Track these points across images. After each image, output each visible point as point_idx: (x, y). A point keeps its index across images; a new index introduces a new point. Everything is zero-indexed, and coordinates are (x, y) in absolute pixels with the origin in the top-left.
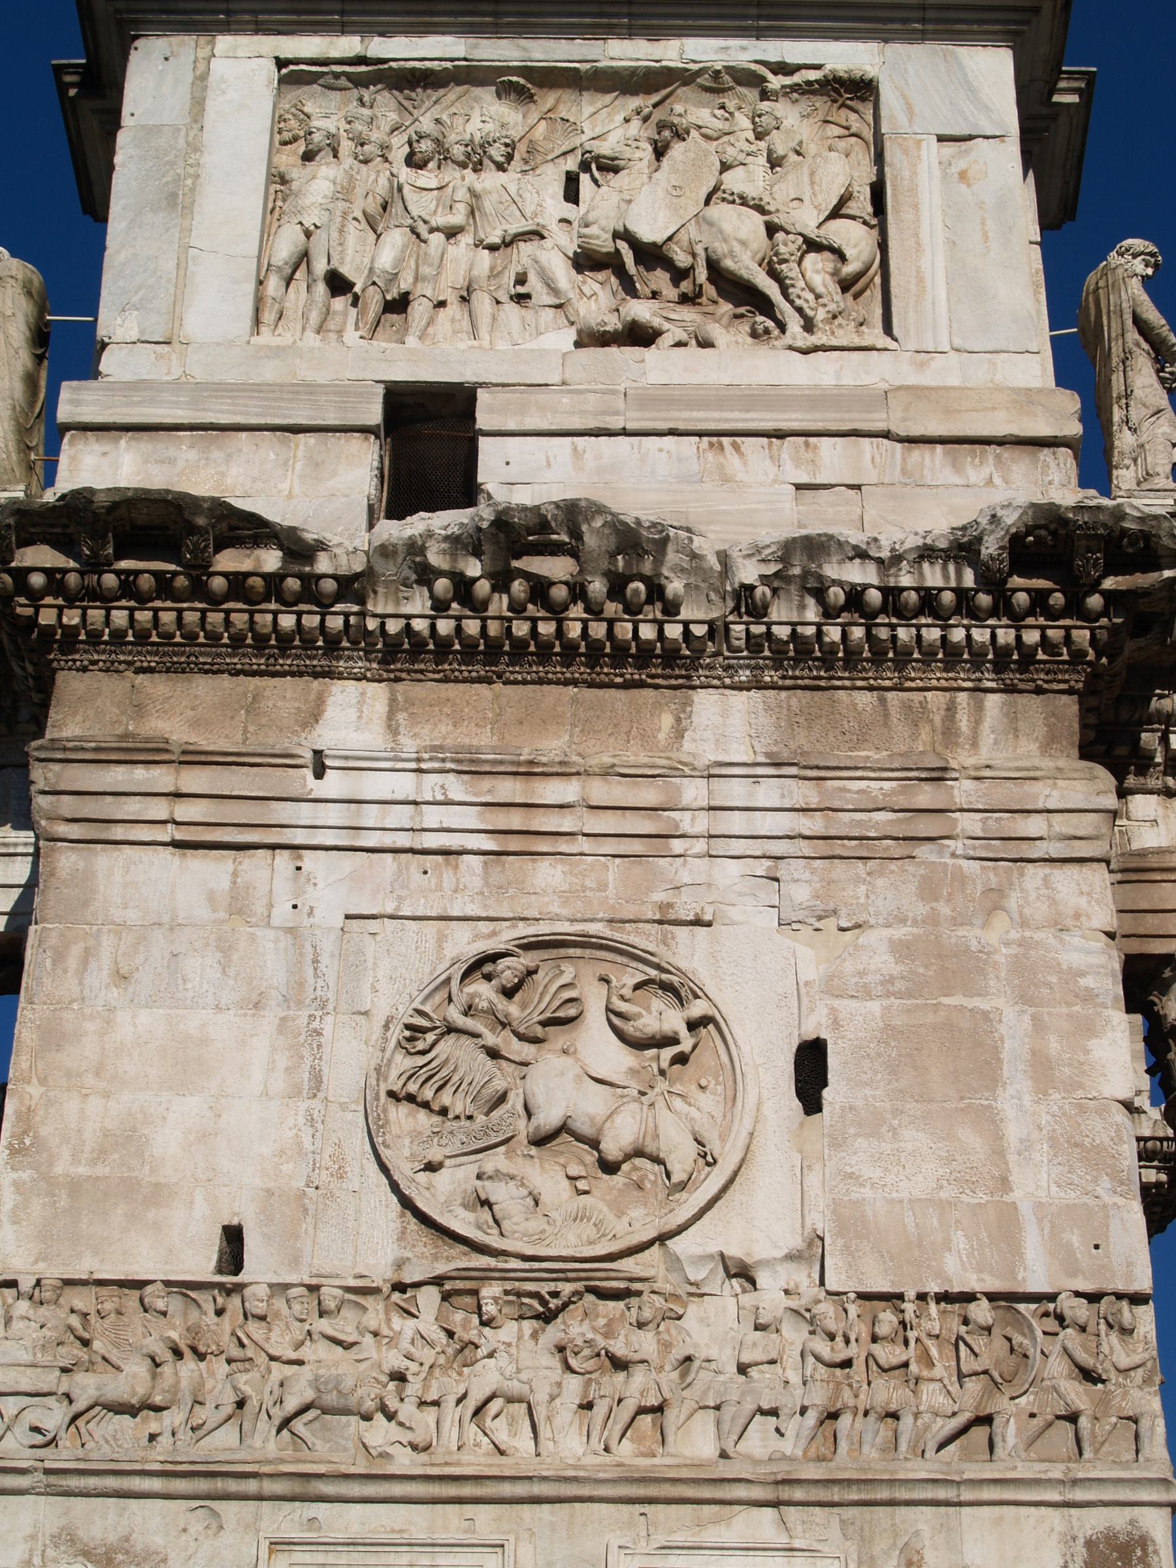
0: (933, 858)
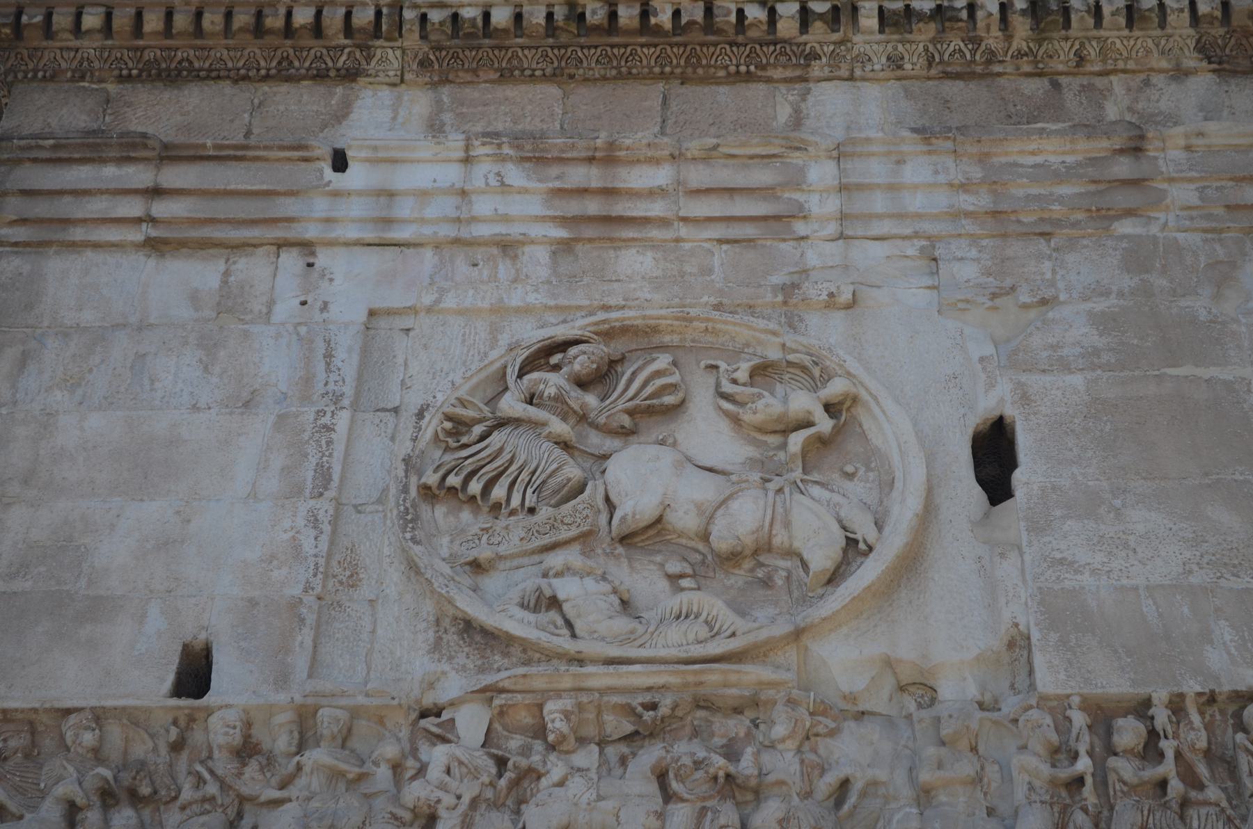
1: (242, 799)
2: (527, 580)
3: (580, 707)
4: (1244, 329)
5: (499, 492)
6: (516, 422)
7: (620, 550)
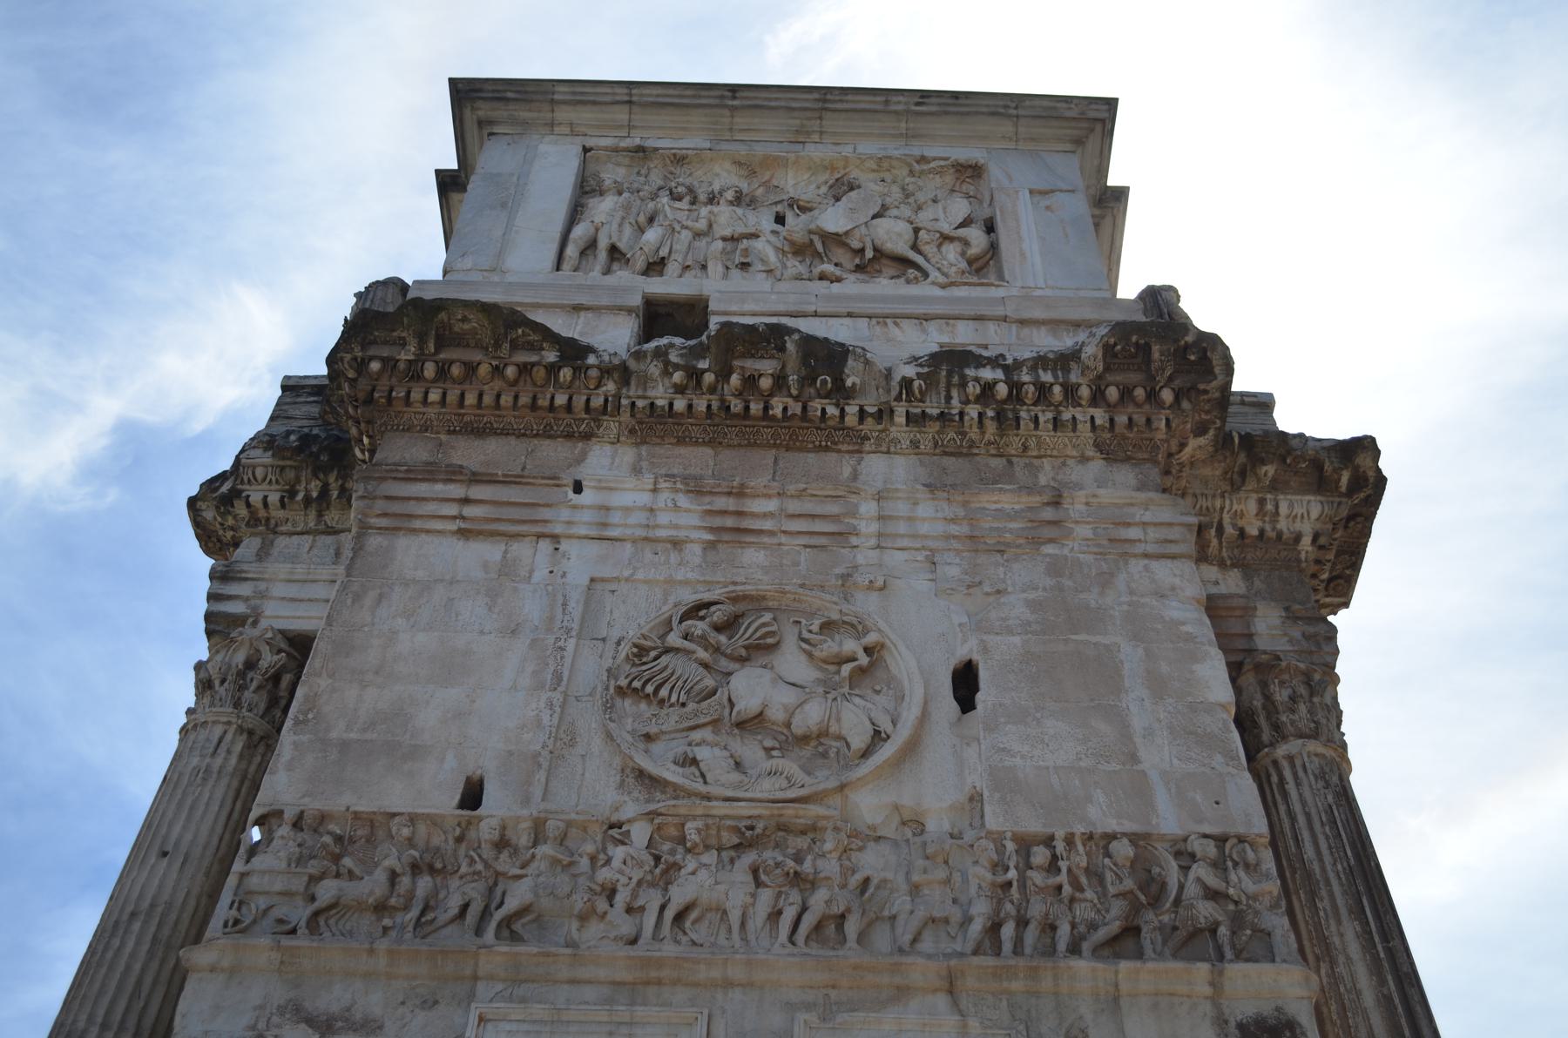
0: (1057, 551)
1: (498, 874)
2: (679, 747)
3: (707, 826)
4: (1117, 614)
5: (664, 693)
6: (677, 650)
7: (736, 731)
